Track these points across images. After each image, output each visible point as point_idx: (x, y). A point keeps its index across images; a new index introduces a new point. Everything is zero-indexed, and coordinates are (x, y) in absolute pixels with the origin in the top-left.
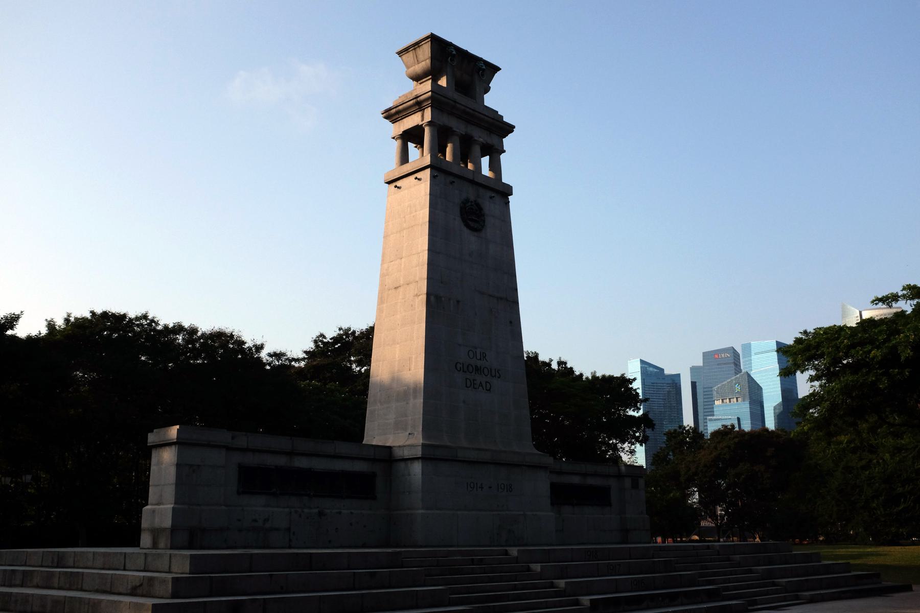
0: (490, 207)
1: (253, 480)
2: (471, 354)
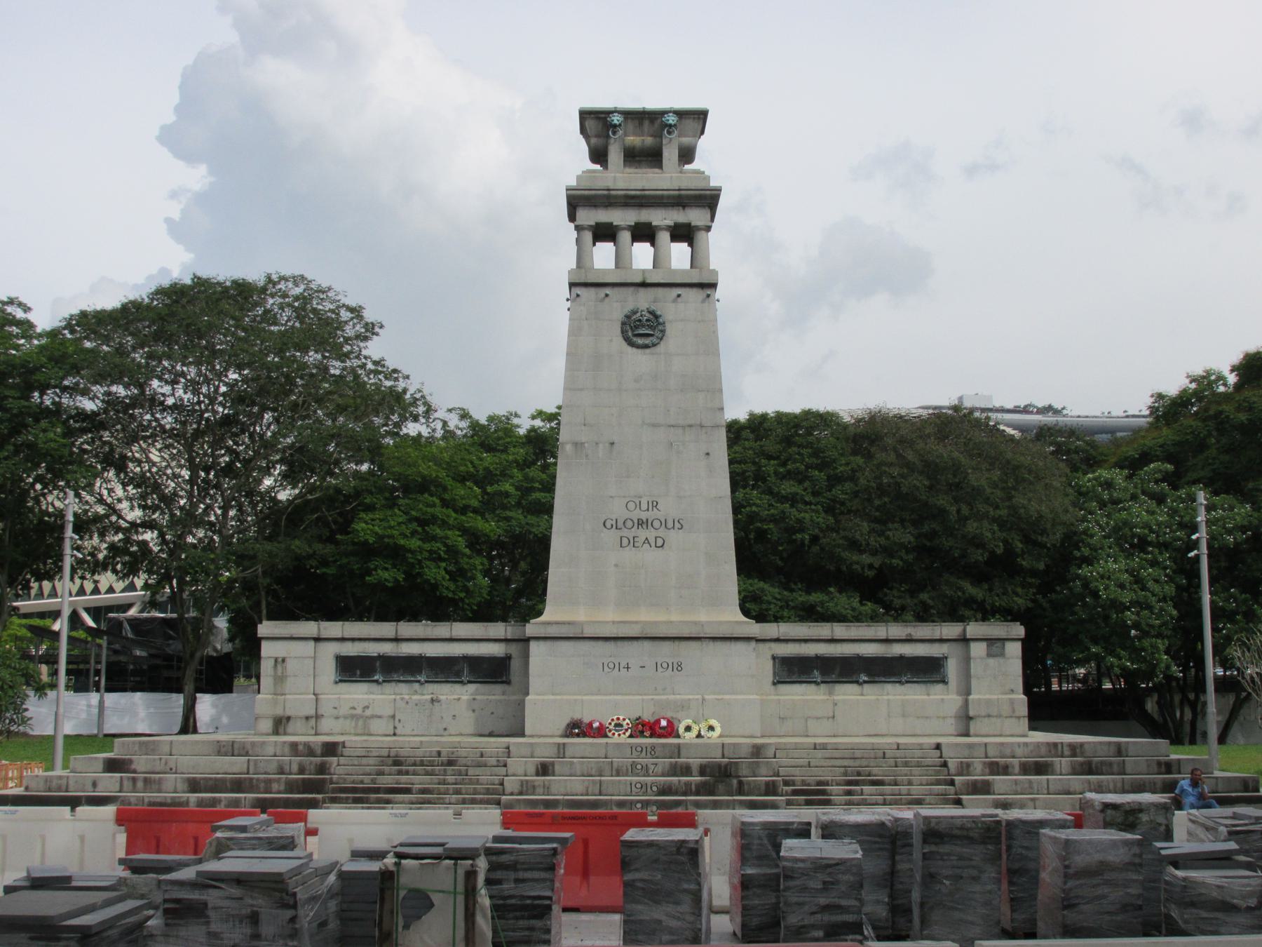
0: (675, 310)
1: (353, 669)
2: (631, 506)
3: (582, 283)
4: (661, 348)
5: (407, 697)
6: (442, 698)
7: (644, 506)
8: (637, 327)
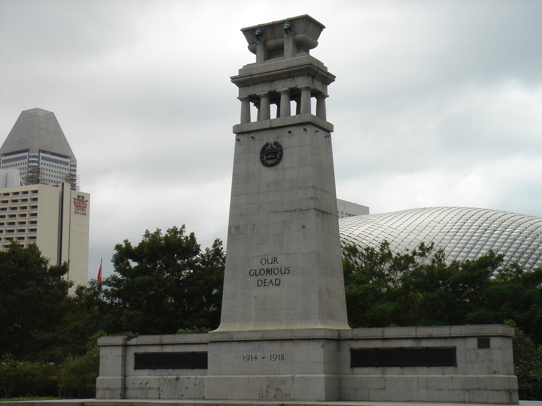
3: (241, 132)
4: (280, 166)
5: (165, 377)
6: (181, 377)
7: (270, 262)
8: (267, 155)
